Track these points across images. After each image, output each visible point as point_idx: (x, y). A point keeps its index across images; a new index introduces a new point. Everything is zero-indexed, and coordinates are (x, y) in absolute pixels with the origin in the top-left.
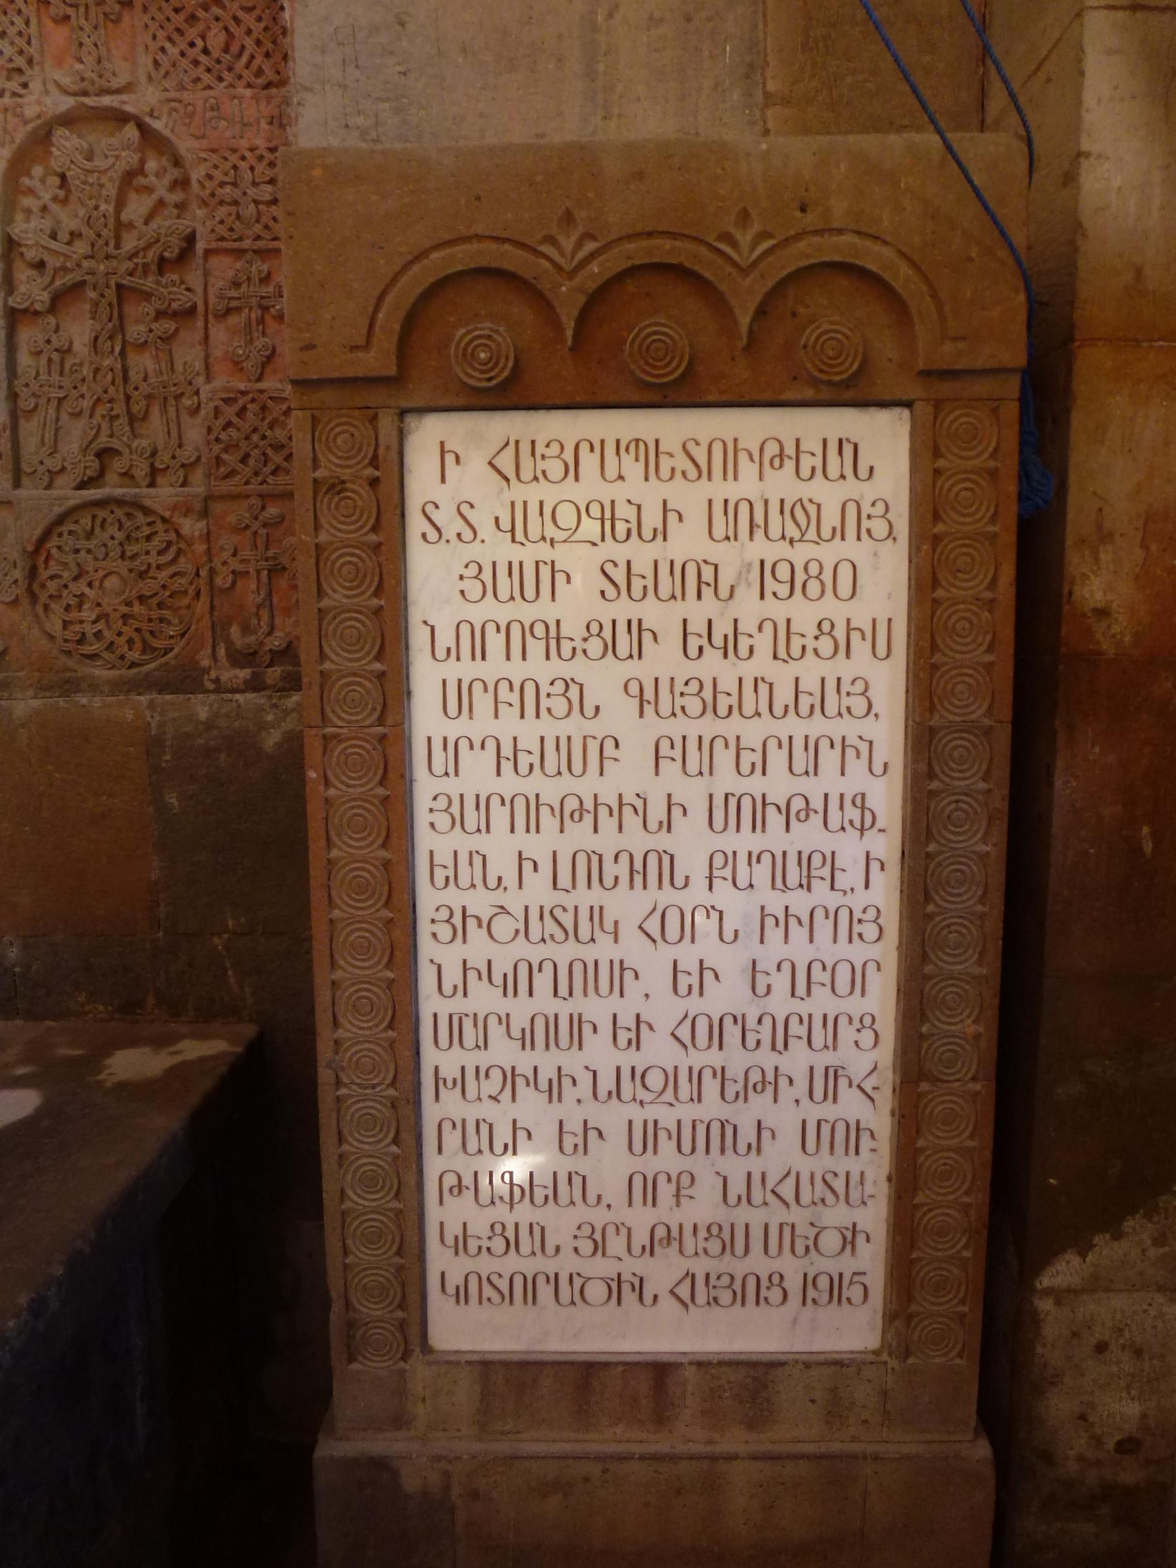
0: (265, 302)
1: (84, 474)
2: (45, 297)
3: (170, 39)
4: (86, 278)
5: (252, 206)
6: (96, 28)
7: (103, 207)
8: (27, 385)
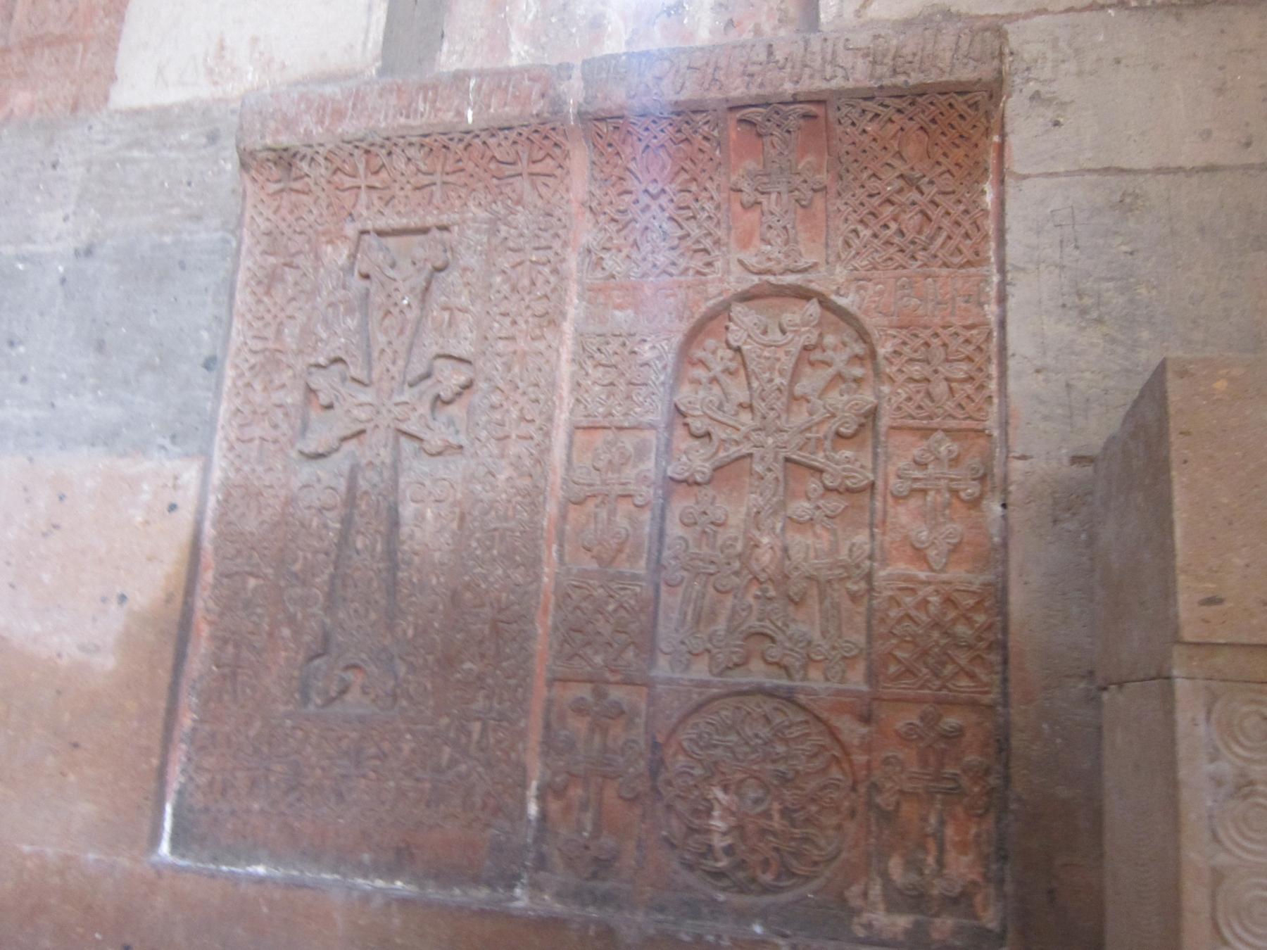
0: (954, 485)
2: (707, 467)
3: (861, 221)
4: (754, 450)
7: (778, 380)
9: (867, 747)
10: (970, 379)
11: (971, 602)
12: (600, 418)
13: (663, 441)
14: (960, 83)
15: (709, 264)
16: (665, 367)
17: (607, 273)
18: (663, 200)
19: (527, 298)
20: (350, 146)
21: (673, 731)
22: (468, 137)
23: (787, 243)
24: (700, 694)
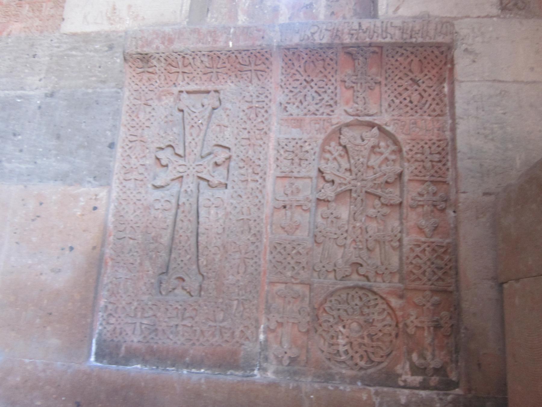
1: (344, 274)
2: (333, 195)
3: (395, 97)
4: (352, 188)
7: (361, 160)
9: (402, 308)
10: (440, 161)
11: (442, 250)
15: (333, 111)
16: (315, 153)
17: (288, 113)
18: (312, 84)
19: (255, 122)
20: (176, 54)
21: (321, 304)
22: (229, 53)
23: (365, 104)
24: (333, 287)
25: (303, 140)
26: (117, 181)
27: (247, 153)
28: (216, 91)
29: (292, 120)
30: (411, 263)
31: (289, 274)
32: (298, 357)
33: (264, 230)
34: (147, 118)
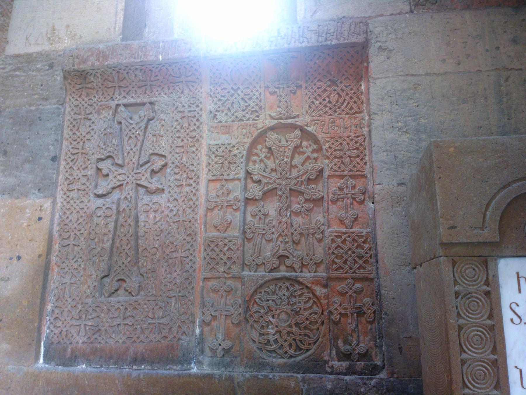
1: (272, 266)
2: (260, 194)
3: (315, 98)
4: (278, 186)
5: (348, 159)
6: (286, 95)
7: (286, 160)
8: (250, 228)
9: (327, 297)
10: (358, 156)
11: (363, 240)
12: (218, 176)
13: (243, 184)
14: (351, 43)
16: (242, 156)
18: (239, 92)
19: (187, 131)
20: (111, 70)
21: (252, 295)
22: (160, 66)
24: (262, 280)
25: (231, 145)
26: (62, 192)
27: (181, 159)
28: (151, 103)
29: (221, 127)
30: (333, 253)
31: (222, 269)
32: (231, 348)
33: (198, 230)
34: (88, 131)
